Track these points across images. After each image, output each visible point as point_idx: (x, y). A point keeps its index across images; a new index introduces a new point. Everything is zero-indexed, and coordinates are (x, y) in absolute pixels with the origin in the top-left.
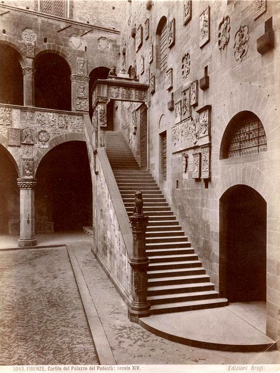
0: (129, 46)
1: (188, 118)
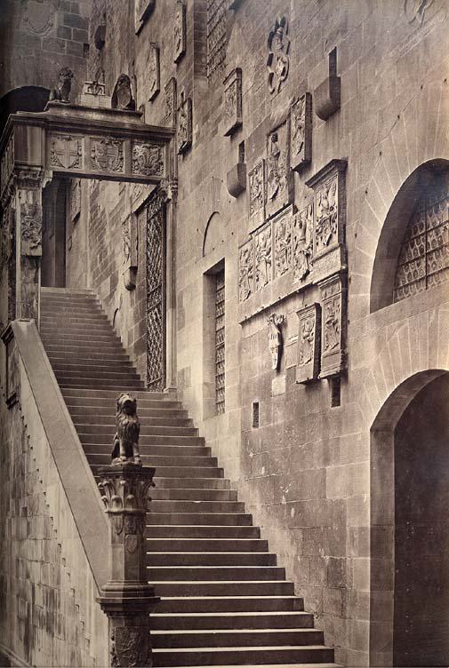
0: (115, 19)
1: (285, 207)
